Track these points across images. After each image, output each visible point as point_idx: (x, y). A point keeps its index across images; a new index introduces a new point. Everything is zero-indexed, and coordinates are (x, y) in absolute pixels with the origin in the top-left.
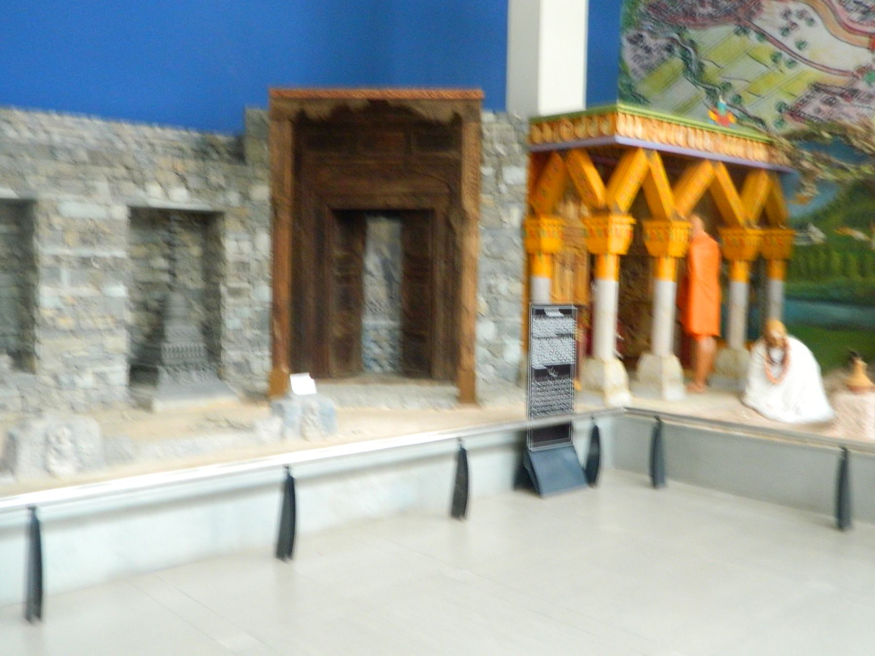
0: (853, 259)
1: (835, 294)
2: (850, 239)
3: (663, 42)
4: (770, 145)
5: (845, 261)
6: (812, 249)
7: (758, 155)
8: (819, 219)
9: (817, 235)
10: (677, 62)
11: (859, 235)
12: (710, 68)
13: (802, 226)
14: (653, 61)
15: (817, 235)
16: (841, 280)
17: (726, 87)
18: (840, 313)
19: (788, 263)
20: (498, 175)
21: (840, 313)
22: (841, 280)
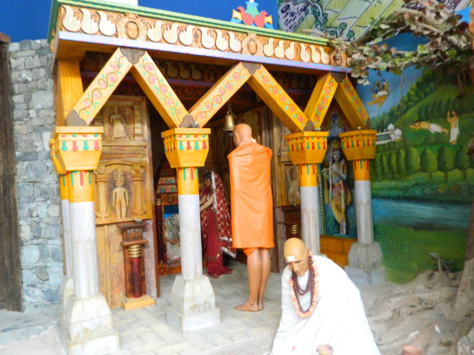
0: (432, 155)
1: (417, 192)
2: (427, 133)
3: (301, 6)
4: (330, 48)
5: (423, 155)
6: (391, 146)
7: (317, 59)
8: (393, 117)
9: (396, 134)
10: (311, 17)
11: (435, 128)
12: (331, 15)
13: (382, 127)
14: (297, 20)
15: (396, 134)
16: (421, 177)
17: (343, 26)
18: (426, 212)
19: (372, 163)
20: (28, 100)
21: (426, 212)
22: (421, 177)
